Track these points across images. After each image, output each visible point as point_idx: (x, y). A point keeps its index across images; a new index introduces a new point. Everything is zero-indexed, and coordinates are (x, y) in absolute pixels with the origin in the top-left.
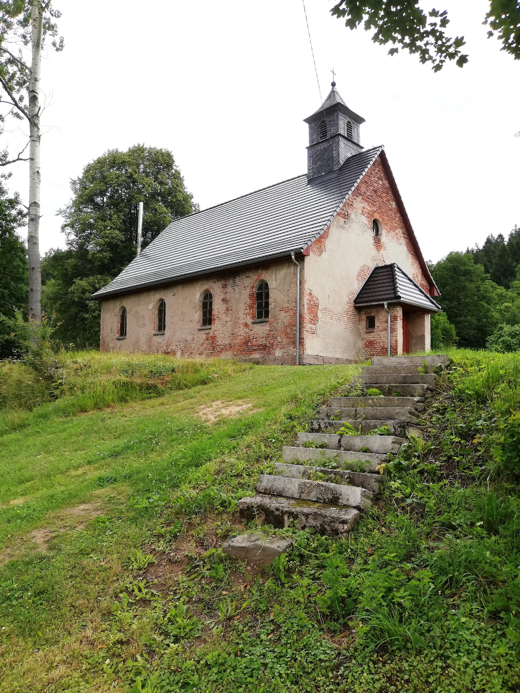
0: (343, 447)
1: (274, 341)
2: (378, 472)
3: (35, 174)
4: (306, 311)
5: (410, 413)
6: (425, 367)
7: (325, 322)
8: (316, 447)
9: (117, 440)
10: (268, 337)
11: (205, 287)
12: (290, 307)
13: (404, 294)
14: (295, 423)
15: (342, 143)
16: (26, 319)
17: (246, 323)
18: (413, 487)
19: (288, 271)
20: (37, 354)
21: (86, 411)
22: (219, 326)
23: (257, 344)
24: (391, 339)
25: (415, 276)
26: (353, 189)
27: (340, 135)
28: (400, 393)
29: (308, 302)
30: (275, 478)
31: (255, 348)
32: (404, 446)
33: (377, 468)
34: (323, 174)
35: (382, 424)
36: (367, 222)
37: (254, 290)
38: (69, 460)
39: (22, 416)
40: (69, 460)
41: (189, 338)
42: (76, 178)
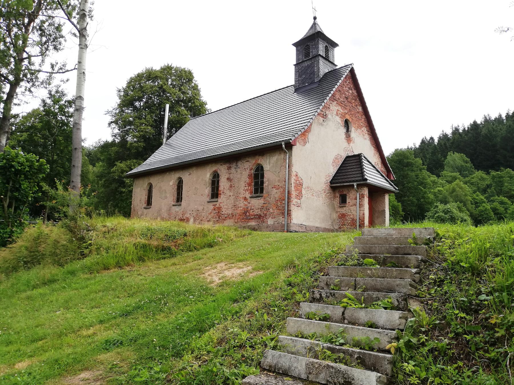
0: (347, 319)
1: (268, 212)
2: (388, 352)
3: (81, 74)
4: (293, 189)
5: (411, 285)
6: (414, 239)
7: (307, 198)
8: (320, 320)
9: (130, 299)
10: (262, 209)
11: (214, 169)
12: (280, 186)
13: (369, 177)
14: (295, 290)
15: (321, 61)
16: (66, 189)
17: (246, 197)
18: (427, 370)
19: (279, 157)
20: (73, 219)
21: (108, 269)
22: (224, 199)
23: (254, 214)
24: (359, 213)
25: (376, 164)
26: (330, 95)
27: (320, 55)
28: (395, 264)
29: (295, 181)
30: (280, 355)
31: (252, 217)
32: (411, 321)
33: (387, 347)
34: (307, 84)
35: (385, 297)
36: (340, 121)
37: (252, 171)
38: (84, 318)
39: (53, 272)
40: (84, 318)
41: (200, 208)
42: (121, 88)
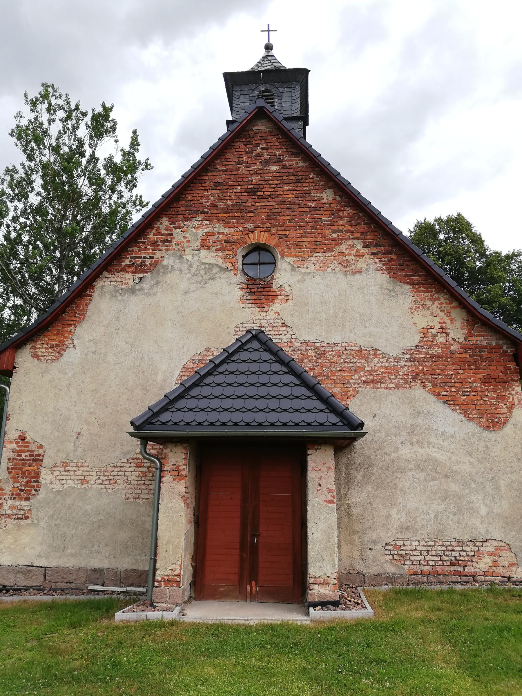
7: (59, 492)
